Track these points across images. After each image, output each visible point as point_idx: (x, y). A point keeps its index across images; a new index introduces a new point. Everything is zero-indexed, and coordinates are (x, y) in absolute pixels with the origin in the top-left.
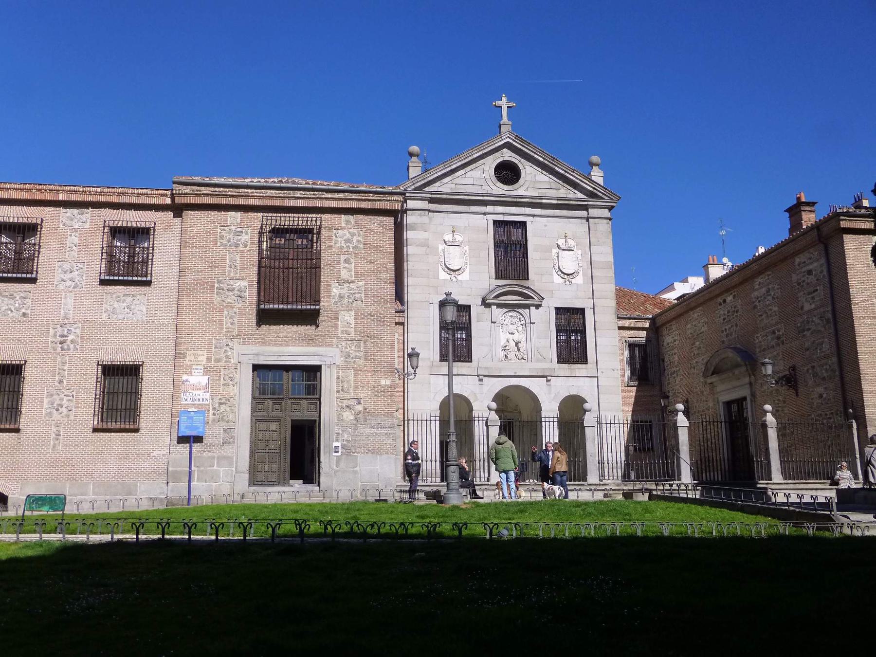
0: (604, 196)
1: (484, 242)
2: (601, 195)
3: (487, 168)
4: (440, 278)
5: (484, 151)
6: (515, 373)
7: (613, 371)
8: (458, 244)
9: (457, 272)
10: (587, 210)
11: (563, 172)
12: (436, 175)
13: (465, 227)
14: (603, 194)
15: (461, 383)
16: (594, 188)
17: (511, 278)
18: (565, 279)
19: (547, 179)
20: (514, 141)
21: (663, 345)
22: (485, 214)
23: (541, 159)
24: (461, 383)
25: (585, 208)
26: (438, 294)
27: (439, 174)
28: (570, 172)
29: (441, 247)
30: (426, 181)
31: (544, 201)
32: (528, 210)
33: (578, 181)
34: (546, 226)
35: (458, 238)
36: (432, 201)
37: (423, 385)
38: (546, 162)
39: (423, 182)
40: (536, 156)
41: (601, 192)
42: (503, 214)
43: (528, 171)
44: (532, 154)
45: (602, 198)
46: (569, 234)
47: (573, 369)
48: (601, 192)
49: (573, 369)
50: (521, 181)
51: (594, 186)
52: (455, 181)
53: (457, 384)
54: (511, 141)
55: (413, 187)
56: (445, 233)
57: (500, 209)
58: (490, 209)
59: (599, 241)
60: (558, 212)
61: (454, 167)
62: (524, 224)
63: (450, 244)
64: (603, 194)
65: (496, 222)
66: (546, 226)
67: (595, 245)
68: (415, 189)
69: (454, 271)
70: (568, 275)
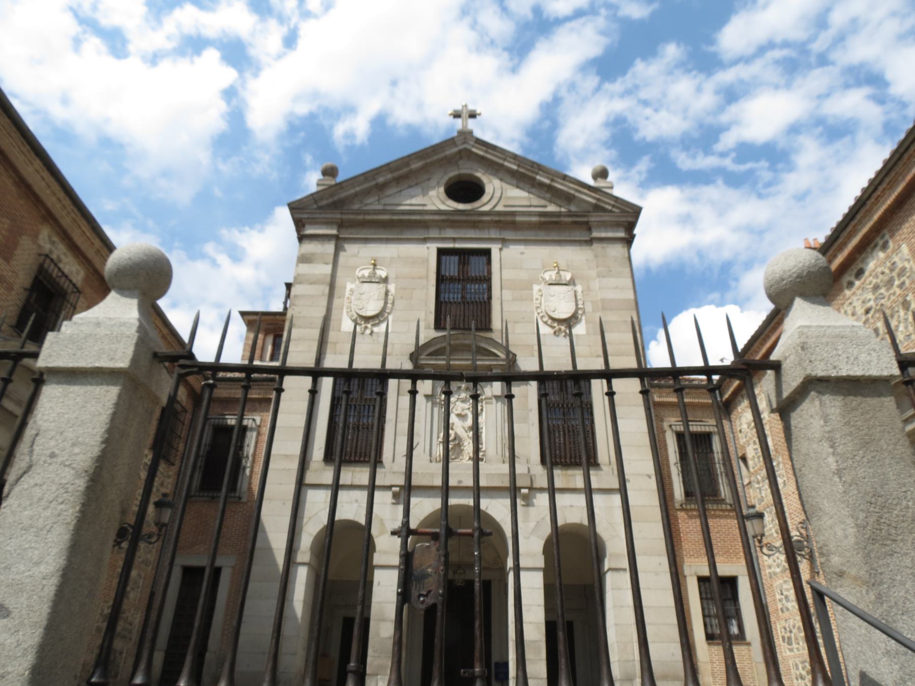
0: (614, 210)
1: (420, 278)
2: (610, 208)
3: (433, 182)
4: (342, 330)
5: (428, 160)
6: (460, 482)
7: (647, 478)
8: (377, 280)
9: (371, 320)
10: (590, 229)
11: (547, 181)
12: (352, 191)
13: (392, 258)
14: (613, 206)
15: (357, 501)
16: (598, 200)
17: (461, 326)
18: (554, 327)
19: (525, 194)
20: (473, 146)
21: (740, 431)
22: (425, 240)
23: (515, 167)
24: (357, 501)
25: (588, 227)
26: (335, 354)
27: (358, 189)
28: (559, 180)
29: (349, 286)
30: (336, 198)
31: (519, 219)
32: (494, 234)
33: (572, 192)
34: (522, 253)
35: (382, 273)
36: (341, 225)
37: (284, 504)
38: (522, 170)
39: (331, 200)
40: (506, 164)
41: (609, 204)
42: (454, 240)
43: (493, 186)
44: (501, 161)
45: (611, 211)
46: (563, 265)
47: (570, 476)
48: (609, 204)
49: (570, 476)
50: (485, 198)
51: (598, 196)
52: (383, 201)
53: (351, 503)
54: (468, 147)
55: (315, 206)
56: (358, 267)
57: (450, 233)
58: (434, 233)
59: (610, 271)
60: (542, 236)
61: (381, 180)
62: (487, 253)
63: (365, 280)
64: (613, 206)
65: (441, 252)
66: (522, 253)
67: (604, 277)
68: (320, 208)
69: (367, 319)
70: (560, 321)
